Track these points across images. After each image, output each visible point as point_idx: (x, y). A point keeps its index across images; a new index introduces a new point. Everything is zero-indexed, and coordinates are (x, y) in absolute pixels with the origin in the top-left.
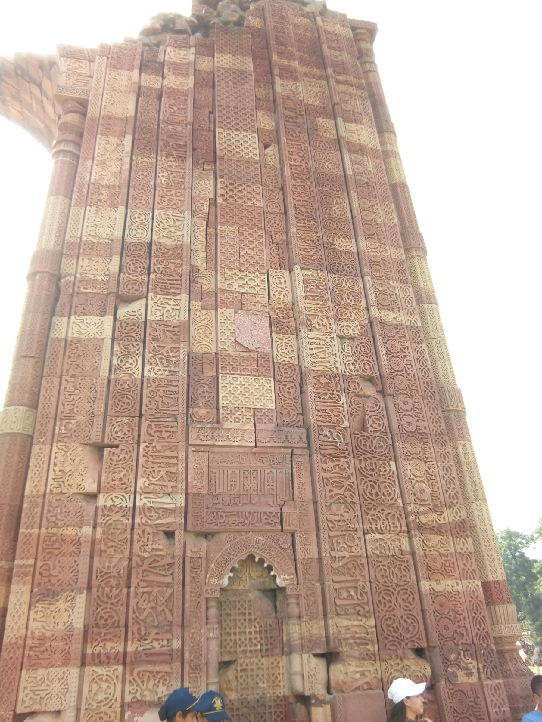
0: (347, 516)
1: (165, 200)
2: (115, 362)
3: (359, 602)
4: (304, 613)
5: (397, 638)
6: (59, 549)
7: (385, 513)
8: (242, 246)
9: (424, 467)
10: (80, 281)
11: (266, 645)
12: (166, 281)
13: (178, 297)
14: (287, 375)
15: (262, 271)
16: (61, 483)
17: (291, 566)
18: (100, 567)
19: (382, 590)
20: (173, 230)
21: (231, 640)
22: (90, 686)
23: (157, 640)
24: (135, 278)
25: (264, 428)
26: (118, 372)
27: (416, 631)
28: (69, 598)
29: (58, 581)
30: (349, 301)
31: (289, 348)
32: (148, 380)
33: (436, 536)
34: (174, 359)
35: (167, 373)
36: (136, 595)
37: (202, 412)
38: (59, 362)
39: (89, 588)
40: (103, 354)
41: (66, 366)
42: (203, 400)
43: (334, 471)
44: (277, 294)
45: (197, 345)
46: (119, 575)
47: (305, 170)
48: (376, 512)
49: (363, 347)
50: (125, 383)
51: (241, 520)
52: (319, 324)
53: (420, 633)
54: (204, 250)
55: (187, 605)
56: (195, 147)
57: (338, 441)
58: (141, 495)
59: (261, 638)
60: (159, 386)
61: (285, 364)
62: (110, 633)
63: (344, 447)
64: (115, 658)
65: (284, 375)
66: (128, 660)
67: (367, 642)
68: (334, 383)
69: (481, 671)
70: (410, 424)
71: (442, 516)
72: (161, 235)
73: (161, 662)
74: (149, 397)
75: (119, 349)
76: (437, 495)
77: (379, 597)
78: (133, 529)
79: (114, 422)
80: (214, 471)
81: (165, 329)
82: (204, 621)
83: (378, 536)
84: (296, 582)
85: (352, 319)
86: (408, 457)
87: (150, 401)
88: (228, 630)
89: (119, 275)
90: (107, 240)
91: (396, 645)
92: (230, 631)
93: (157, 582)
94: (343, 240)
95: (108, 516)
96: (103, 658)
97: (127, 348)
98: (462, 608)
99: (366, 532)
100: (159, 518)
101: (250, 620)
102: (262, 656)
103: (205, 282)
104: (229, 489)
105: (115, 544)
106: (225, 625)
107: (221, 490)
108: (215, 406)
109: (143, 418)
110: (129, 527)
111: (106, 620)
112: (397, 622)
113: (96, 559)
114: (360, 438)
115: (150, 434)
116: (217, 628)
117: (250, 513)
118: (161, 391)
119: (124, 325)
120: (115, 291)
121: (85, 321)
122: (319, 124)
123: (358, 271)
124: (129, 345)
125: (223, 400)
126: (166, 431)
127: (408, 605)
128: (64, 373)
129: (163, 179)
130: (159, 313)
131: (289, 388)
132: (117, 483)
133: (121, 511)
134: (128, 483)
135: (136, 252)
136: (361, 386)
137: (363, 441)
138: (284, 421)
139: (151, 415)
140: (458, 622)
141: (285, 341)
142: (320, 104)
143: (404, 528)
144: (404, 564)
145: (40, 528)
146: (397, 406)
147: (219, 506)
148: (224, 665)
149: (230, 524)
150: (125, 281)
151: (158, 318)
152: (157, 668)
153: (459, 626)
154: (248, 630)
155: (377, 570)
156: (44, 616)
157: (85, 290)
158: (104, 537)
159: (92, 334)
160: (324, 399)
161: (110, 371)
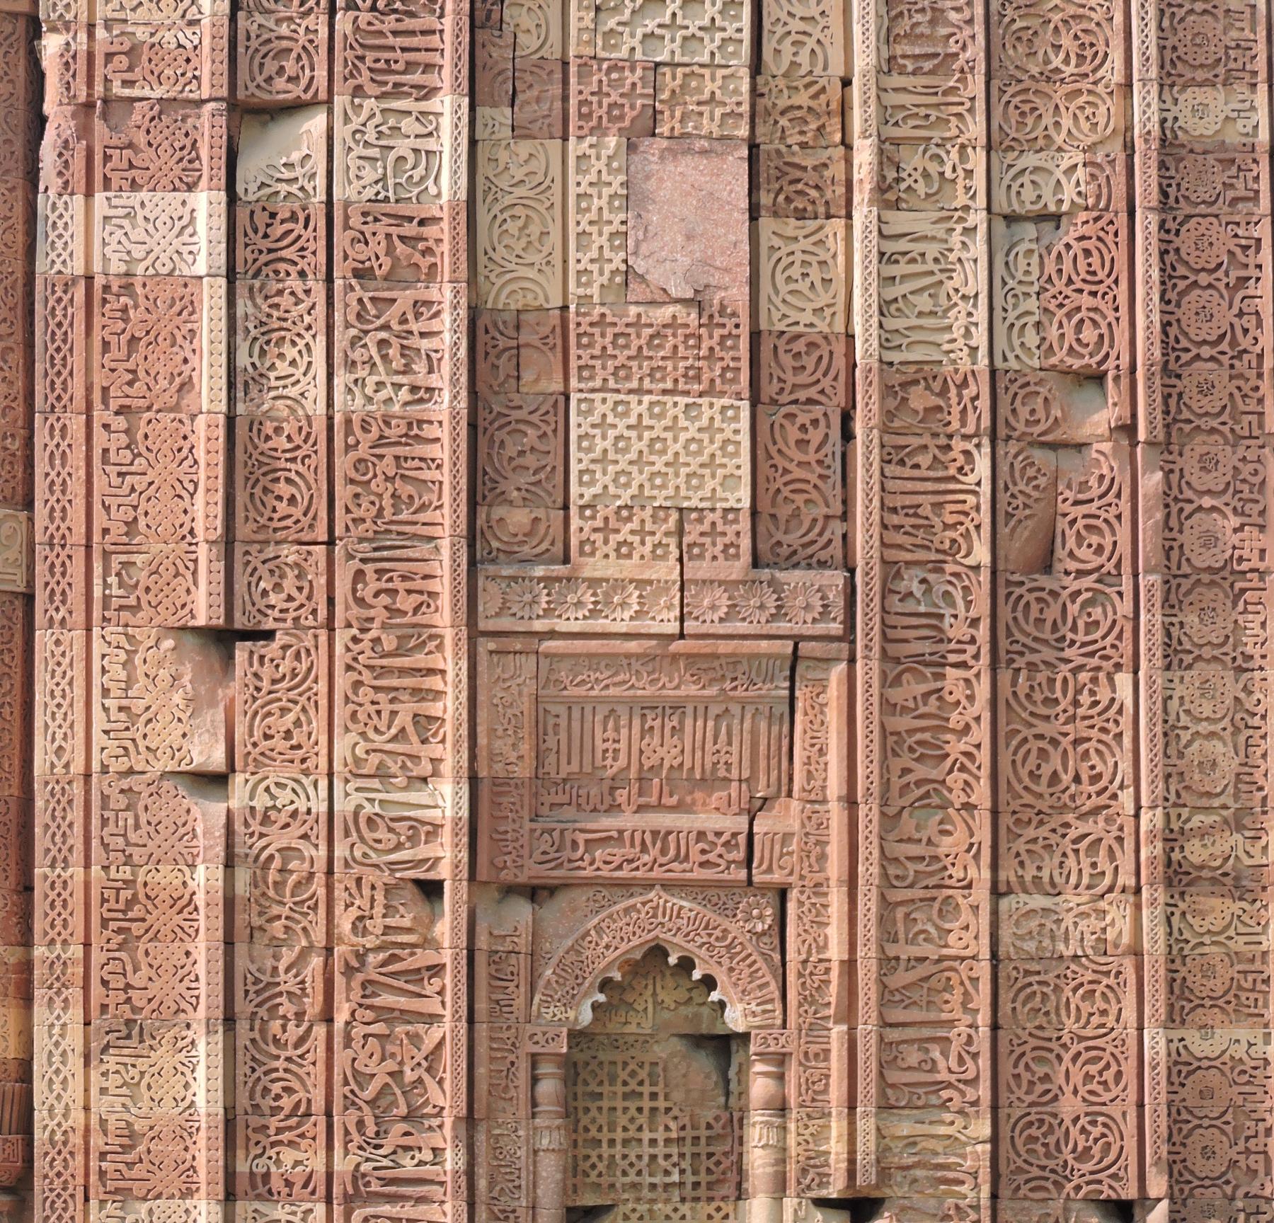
2: (243, 360)
4: (793, 1101)
5: (1053, 1171)
6: (144, 920)
7: (1073, 833)
9: (1232, 688)
10: (109, 56)
11: (695, 1173)
12: (391, 40)
14: (803, 378)
16: (129, 744)
17: (768, 978)
18: (253, 968)
19: (1027, 1048)
21: (600, 1157)
23: (407, 1148)
25: (707, 576)
26: (254, 392)
27: (1112, 1157)
28: (180, 1044)
29: (150, 1000)
32: (348, 422)
33: (1228, 901)
34: (425, 344)
35: (404, 394)
38: (77, 361)
41: (99, 380)
44: (787, 46)
45: (499, 282)
46: (303, 989)
48: (1043, 831)
49: (1087, 253)
51: (630, 852)
58: (347, 781)
59: (682, 1155)
60: (381, 442)
61: (798, 336)
62: (290, 1128)
64: (305, 1186)
65: (791, 379)
66: (336, 1190)
67: (961, 1176)
68: (956, 410)
70: (1210, 540)
74: (352, 481)
75: (251, 310)
77: (1016, 1066)
78: (330, 872)
79: (255, 562)
80: (554, 709)
82: (523, 1112)
83: (1038, 901)
84: (779, 1022)
87: (357, 496)
88: (593, 1132)
89: (233, 18)
91: (1047, 1189)
92: (599, 1136)
93: (402, 1011)
95: (262, 835)
96: (276, 1184)
97: (277, 306)
99: (1002, 888)
100: (399, 847)
101: (654, 1110)
102: (683, 1200)
104: (599, 763)
106: (585, 1121)
107: (575, 767)
108: (560, 500)
110: (321, 865)
111: (278, 1097)
112: (1060, 1133)
113: (241, 949)
115: (361, 602)
116: (558, 1128)
117: (655, 833)
118: (389, 460)
119: (262, 219)
120: (224, 92)
121: (140, 214)
124: (280, 293)
125: (581, 483)
126: (409, 592)
127: (1100, 1089)
128: (97, 404)
130: (370, 174)
131: (803, 428)
132: (279, 743)
133: (295, 825)
136: (1056, 412)
137: (1035, 608)
138: (779, 543)
140: (1247, 1139)
141: (805, 244)
144: (1105, 981)
145: (87, 866)
146: (1175, 478)
150: (254, 44)
151: (369, 193)
153: (1248, 1151)
154: (646, 1136)
155: (1022, 996)
156: (125, 1084)
157: (127, 92)
158: (257, 892)
159: (164, 258)
160: (917, 466)
161: (231, 385)
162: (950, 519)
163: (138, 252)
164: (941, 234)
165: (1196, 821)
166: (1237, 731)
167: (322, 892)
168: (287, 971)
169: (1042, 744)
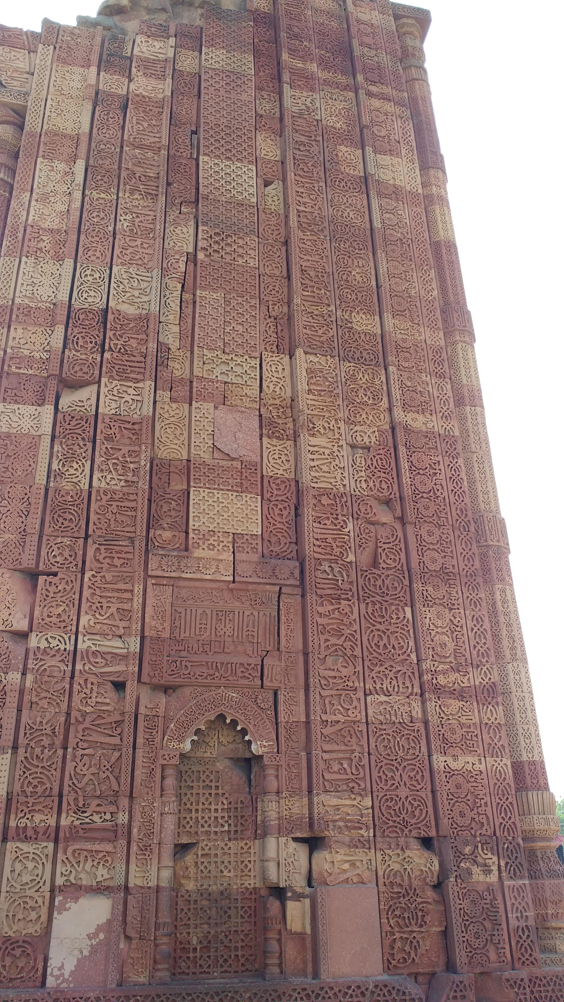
0: (345, 672)
1: (128, 252)
2: (55, 466)
3: (353, 777)
5: (399, 823)
7: (394, 670)
8: (228, 319)
9: (448, 615)
10: (11, 358)
11: (236, 826)
12: (125, 363)
13: (140, 385)
14: (280, 493)
15: (254, 354)
17: (271, 730)
19: (383, 764)
20: (136, 293)
21: (191, 818)
22: (13, 865)
23: (98, 813)
24: (83, 357)
26: (58, 479)
27: (424, 816)
30: (366, 399)
31: (284, 458)
32: (98, 491)
34: (132, 466)
35: (122, 483)
36: (74, 756)
37: (167, 535)
39: (15, 748)
40: (40, 456)
42: (169, 520)
43: (332, 616)
44: (271, 385)
45: (163, 449)
46: (54, 733)
47: (318, 219)
48: (382, 669)
49: (381, 459)
50: (68, 493)
51: (211, 672)
52: (324, 428)
53: (427, 819)
54: (177, 322)
55: (137, 773)
56: (170, 180)
57: (340, 578)
58: (85, 636)
59: (229, 817)
60: (112, 499)
61: (278, 478)
63: (346, 586)
64: (44, 834)
65: (275, 492)
66: (61, 835)
68: (339, 505)
69: (503, 868)
70: (434, 561)
71: (467, 677)
72: (120, 300)
73: (102, 840)
75: (60, 449)
76: (462, 650)
78: (72, 677)
80: (179, 610)
81: (122, 426)
82: (158, 793)
83: (383, 698)
84: (276, 750)
85: (368, 423)
86: (428, 602)
87: (99, 519)
88: (188, 805)
89: (63, 352)
90: (48, 304)
92: (191, 807)
94: (364, 317)
96: (30, 833)
97: (72, 449)
98: (484, 792)
99: (368, 692)
100: (107, 665)
101: (217, 794)
102: (230, 840)
103: (177, 366)
104: (197, 633)
105: (49, 695)
106: (184, 800)
107: (187, 634)
108: (184, 529)
109: (90, 541)
110: (68, 674)
111: (36, 786)
112: (400, 804)
113: (25, 712)
114: (369, 576)
117: (222, 664)
119: (68, 418)
120: (57, 373)
121: (17, 411)
122: (340, 154)
123: (381, 360)
124: (74, 444)
125: (194, 520)
127: (415, 783)
129: (126, 224)
130: (114, 405)
132: (54, 619)
134: (67, 621)
135: (87, 322)
137: (372, 581)
138: (272, 551)
139: (99, 537)
140: (478, 807)
141: (279, 448)
142: (344, 126)
143: (417, 690)
146: (419, 537)
147: (184, 654)
148: (181, 849)
149: (197, 676)
150: (71, 360)
151: (113, 412)
152: (97, 847)
154: (213, 807)
155: (379, 740)
157: (17, 371)
158: (36, 686)
159: (25, 428)
161: (48, 477)
162: (339, 544)
163: (14, 425)
164: (330, 447)
165: (440, 668)
166: (452, 632)
167: (67, 686)
168: (46, 724)
169: (379, 633)
